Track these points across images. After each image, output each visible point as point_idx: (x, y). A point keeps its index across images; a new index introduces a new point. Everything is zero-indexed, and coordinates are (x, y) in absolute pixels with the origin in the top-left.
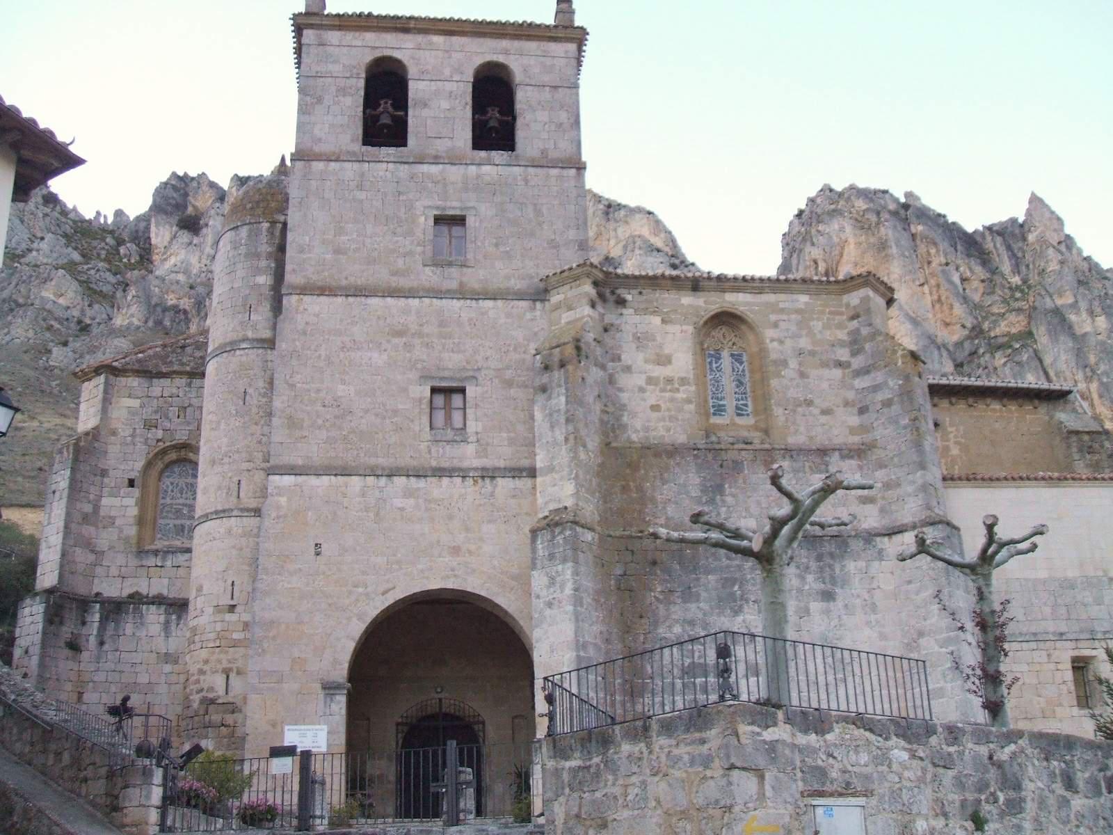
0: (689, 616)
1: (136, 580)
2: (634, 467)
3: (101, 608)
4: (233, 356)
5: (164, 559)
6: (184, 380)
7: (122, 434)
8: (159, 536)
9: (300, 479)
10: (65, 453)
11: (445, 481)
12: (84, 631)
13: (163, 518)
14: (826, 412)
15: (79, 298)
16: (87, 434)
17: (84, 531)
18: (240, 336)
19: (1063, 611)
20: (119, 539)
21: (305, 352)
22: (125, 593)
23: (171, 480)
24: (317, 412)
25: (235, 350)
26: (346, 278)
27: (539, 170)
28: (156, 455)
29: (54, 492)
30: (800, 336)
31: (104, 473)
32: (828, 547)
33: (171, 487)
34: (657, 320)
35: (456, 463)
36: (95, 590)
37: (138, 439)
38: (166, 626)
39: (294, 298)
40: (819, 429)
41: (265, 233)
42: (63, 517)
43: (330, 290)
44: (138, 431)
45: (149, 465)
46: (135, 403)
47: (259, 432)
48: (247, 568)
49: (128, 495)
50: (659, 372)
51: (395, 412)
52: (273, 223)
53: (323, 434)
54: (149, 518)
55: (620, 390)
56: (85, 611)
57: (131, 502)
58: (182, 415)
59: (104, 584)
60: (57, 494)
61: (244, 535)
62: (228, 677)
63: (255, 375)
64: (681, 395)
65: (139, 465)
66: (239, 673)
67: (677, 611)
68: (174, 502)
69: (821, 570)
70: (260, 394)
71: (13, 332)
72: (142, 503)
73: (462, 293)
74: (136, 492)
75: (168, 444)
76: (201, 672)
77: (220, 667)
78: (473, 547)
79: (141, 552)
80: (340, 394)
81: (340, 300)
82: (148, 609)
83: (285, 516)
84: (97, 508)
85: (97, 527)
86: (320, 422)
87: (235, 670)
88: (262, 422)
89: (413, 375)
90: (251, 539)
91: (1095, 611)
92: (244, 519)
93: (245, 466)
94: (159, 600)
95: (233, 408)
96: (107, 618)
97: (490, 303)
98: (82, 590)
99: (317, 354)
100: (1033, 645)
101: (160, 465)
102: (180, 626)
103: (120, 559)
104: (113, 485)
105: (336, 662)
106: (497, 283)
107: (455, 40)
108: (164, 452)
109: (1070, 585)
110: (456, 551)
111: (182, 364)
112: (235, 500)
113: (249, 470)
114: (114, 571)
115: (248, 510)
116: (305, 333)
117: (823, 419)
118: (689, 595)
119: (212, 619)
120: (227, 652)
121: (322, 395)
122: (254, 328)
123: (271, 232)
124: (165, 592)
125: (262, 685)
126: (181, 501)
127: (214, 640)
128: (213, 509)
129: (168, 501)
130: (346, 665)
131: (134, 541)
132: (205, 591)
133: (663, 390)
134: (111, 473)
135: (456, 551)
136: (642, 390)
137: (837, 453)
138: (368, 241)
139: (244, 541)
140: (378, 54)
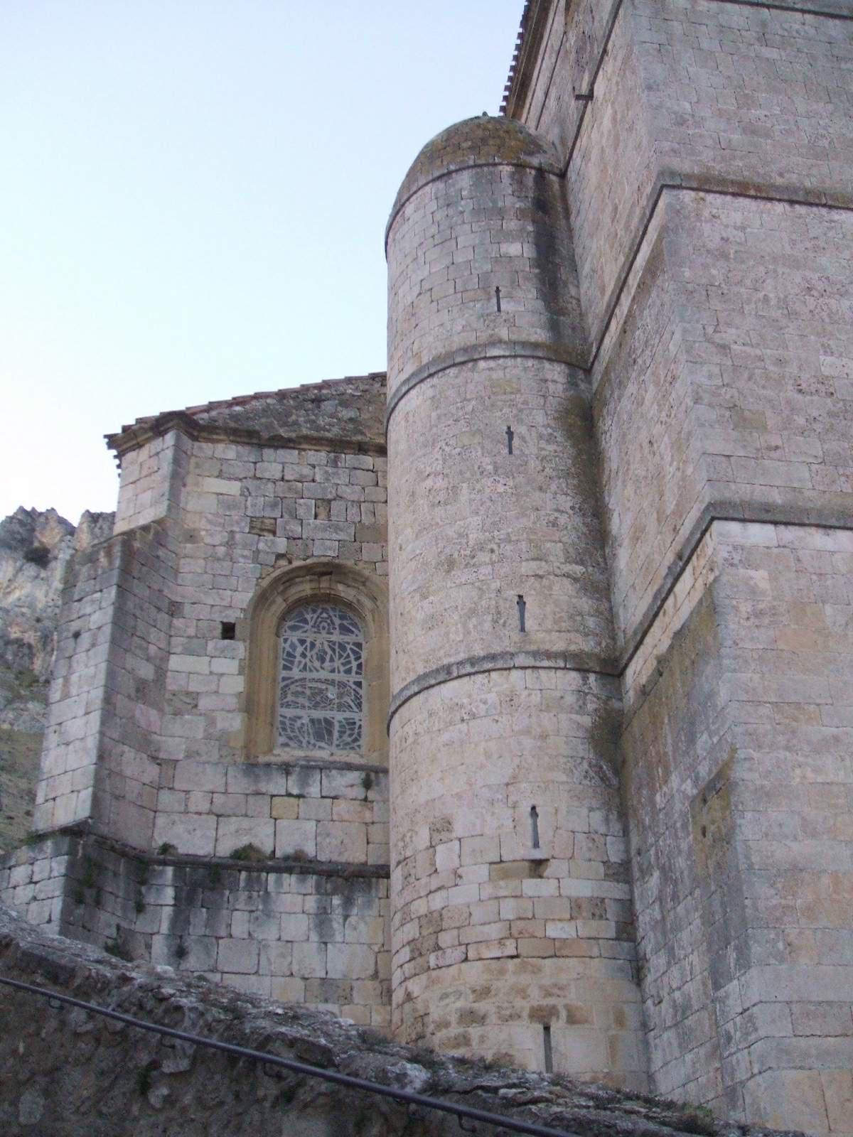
1: (246, 823)
3: (175, 876)
4: (473, 370)
5: (304, 782)
6: (323, 454)
7: (208, 540)
8: (282, 740)
9: (789, 534)
10: (103, 560)
12: (141, 925)
13: (288, 705)
16: (145, 528)
17: (137, 713)
18: (484, 337)
20: (208, 737)
21: (735, 289)
22: (226, 848)
23: (299, 634)
24: (788, 402)
25: (475, 360)
26: (781, 175)
28: (277, 581)
29: (77, 635)
31: (174, 609)
33: (300, 649)
36: (159, 841)
37: (238, 551)
38: (322, 919)
41: (506, 181)
42: (101, 678)
43: (758, 188)
44: (238, 536)
45: (262, 600)
46: (233, 488)
47: (550, 505)
48: (563, 778)
49: (222, 654)
52: (520, 167)
54: (262, 701)
56: (143, 882)
57: (228, 666)
58: (323, 514)
59: (179, 829)
60: (85, 639)
61: (545, 707)
62: (547, 1029)
63: (525, 403)
65: (245, 597)
66: (572, 1020)
68: (308, 675)
70: (541, 437)
72: (250, 668)
74: (240, 648)
75: (296, 563)
76: (471, 1017)
77: (523, 1005)
79: (252, 768)
80: (826, 371)
81: (780, 208)
82: (279, 883)
83: (774, 612)
84: (161, 673)
85: (161, 710)
86: (801, 421)
87: (563, 1014)
88: (554, 487)
90: (563, 717)
92: (542, 673)
93: (528, 568)
94: (298, 864)
95: (488, 460)
96: (190, 900)
98: (135, 838)
99: (761, 295)
101: (279, 605)
102: (353, 920)
103: (212, 779)
104: (191, 631)
108: (287, 579)
111: (318, 429)
112: (516, 636)
113: (541, 577)
114: (199, 801)
115: (549, 655)
116: (725, 256)
119: (488, 891)
120: (537, 970)
121: (792, 369)
122: (511, 323)
123: (518, 178)
124: (310, 850)
125: (803, 1042)
126: (324, 675)
127: (501, 942)
128: (461, 656)
129: (296, 673)
131: (238, 743)
132: (458, 830)
134: (187, 609)
138: (804, 123)
139: (547, 720)
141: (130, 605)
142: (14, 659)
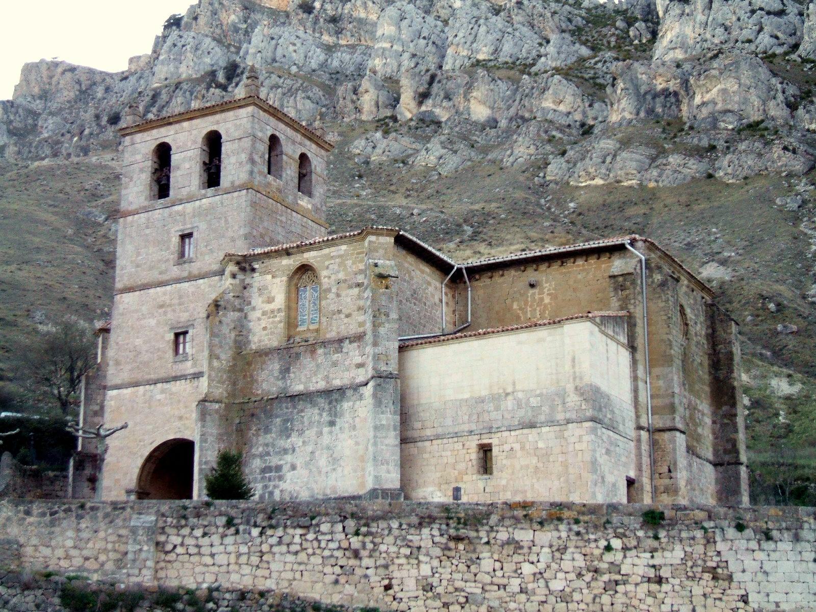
0: (266, 441)
2: (249, 364)
9: (120, 391)
11: (178, 382)
14: (348, 316)
15: (579, 100)
19: (475, 417)
27: (229, 195)
30: (338, 272)
32: (335, 396)
34: (269, 277)
35: (183, 373)
39: (119, 296)
40: (343, 327)
50: (268, 307)
51: (159, 350)
53: (129, 367)
55: (250, 321)
64: (277, 319)
67: (261, 440)
69: (330, 409)
71: (516, 152)
73: (191, 278)
78: (188, 415)
81: (137, 293)
89: (167, 328)
91: (494, 415)
97: (201, 281)
100: (456, 439)
105: (131, 480)
106: (206, 269)
107: (195, 122)
109: (482, 400)
110: (181, 418)
117: (346, 320)
118: (267, 430)
133: (269, 318)
135: (181, 418)
136: (259, 319)
137: (348, 341)
140: (158, 142)
141: (89, 392)
142: (663, 111)
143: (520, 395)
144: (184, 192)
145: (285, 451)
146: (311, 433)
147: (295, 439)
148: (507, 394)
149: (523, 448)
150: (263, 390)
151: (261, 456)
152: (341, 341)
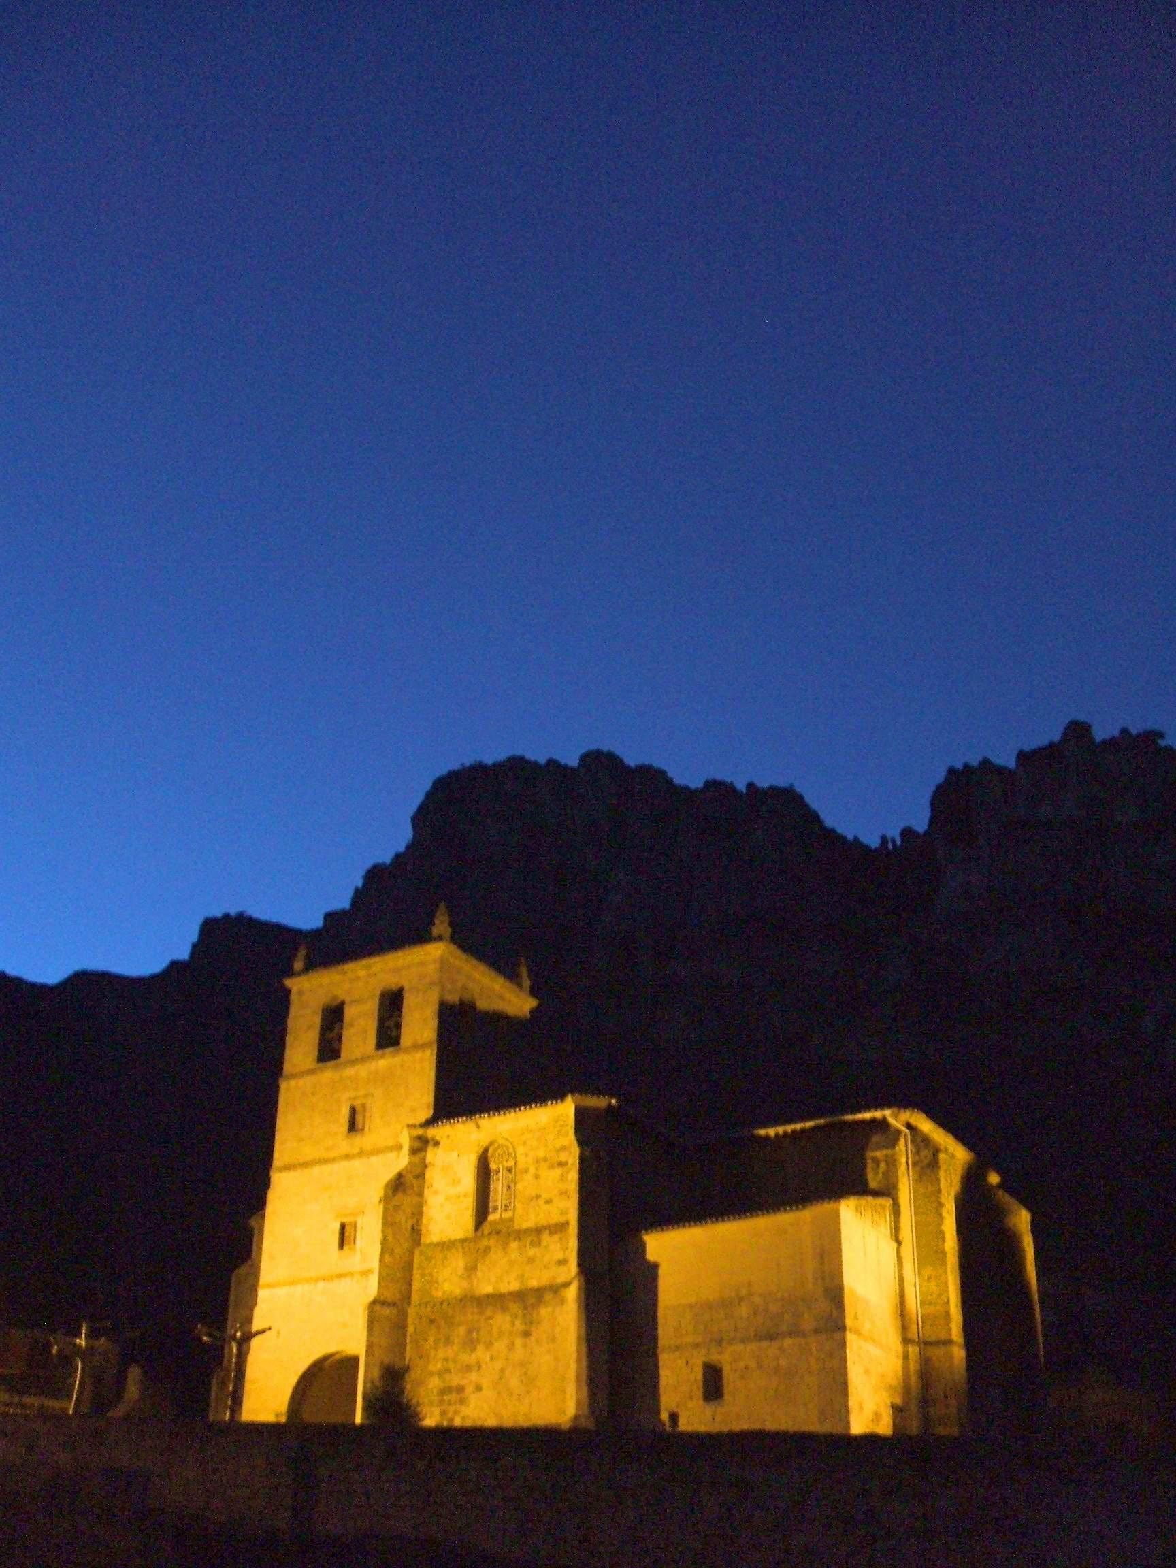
14: (549, 1202)
67: (441, 1354)
69: (524, 1315)
117: (546, 1207)
118: (448, 1341)
130: (287, 1403)
137: (547, 1232)
143: (757, 1300)
144: (357, 1053)
145: (468, 1368)
146: (500, 1346)
147: (481, 1353)
148: (741, 1299)
149: (760, 1367)
150: (444, 1292)
151: (440, 1374)
152: (538, 1231)
